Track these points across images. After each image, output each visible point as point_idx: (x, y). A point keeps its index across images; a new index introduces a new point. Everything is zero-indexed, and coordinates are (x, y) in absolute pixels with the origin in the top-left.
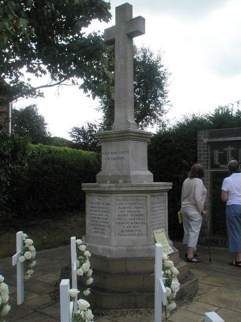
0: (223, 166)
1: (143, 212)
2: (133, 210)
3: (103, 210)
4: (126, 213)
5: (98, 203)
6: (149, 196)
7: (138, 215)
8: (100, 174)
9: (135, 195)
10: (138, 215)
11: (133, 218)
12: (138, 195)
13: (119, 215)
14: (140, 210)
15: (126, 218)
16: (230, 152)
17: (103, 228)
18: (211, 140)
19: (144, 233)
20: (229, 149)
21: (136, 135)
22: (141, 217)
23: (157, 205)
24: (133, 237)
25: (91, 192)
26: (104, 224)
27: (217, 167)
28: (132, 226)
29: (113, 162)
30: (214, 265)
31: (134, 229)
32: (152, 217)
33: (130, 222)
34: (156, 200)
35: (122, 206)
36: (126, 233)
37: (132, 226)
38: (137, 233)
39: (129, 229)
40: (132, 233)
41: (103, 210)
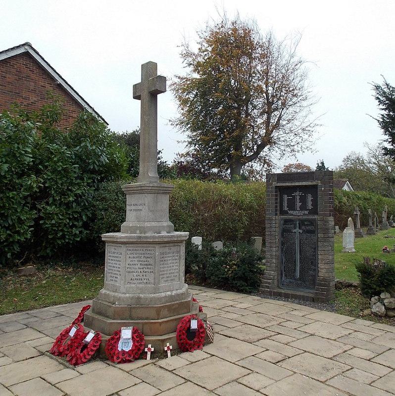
0: (291, 212)
1: (151, 261)
2: (142, 259)
3: (117, 259)
4: (136, 263)
5: (114, 253)
6: (157, 246)
7: (147, 265)
8: (124, 224)
9: (145, 245)
10: (147, 265)
11: (142, 267)
12: (148, 245)
13: (129, 264)
14: (148, 259)
15: (136, 267)
16: (298, 197)
17: (116, 276)
18: (279, 185)
19: (152, 281)
20: (297, 194)
21: (157, 188)
22: (149, 267)
23: (167, 255)
24: (141, 286)
25: (110, 242)
26: (117, 273)
27: (286, 213)
28: (141, 274)
29: (134, 213)
30: (307, 303)
31: (143, 278)
32: (162, 266)
33: (139, 270)
34: (167, 250)
35: (132, 256)
36: (135, 281)
37: (141, 274)
38: (145, 281)
39: (138, 277)
40: (140, 281)
41: (117, 259)
